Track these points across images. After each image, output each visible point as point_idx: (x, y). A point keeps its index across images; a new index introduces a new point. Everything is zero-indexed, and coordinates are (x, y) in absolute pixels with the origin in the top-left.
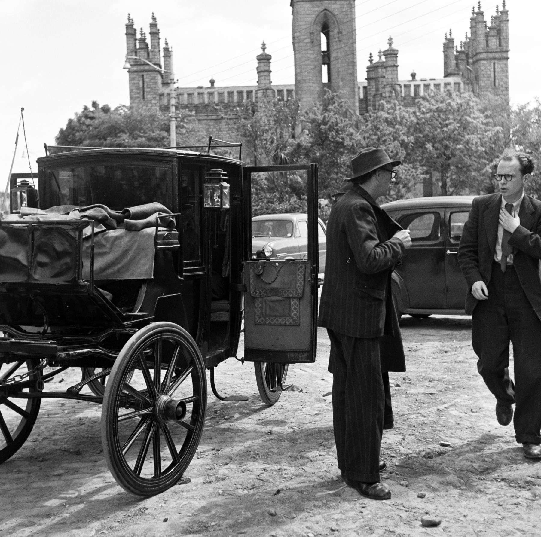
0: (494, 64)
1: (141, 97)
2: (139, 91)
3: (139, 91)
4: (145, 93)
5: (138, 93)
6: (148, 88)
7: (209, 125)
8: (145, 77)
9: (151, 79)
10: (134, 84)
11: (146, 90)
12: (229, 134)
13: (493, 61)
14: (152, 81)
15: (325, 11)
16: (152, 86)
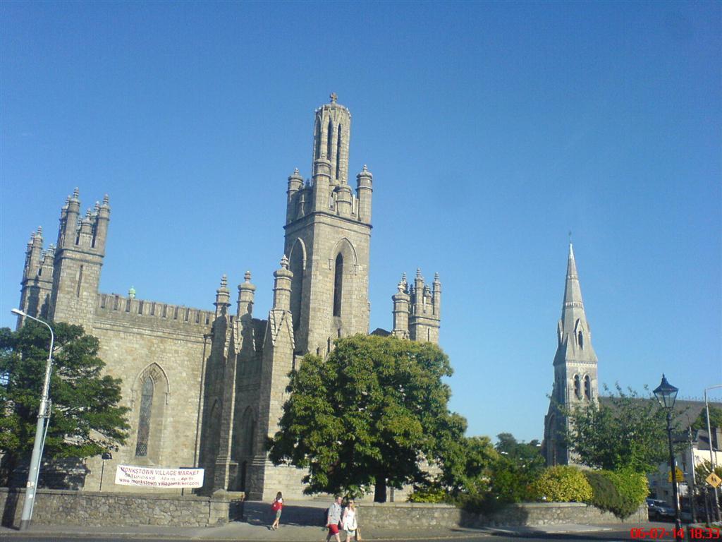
1: (76, 293)
2: (73, 284)
4: (81, 288)
5: (73, 287)
6: (85, 282)
7: (152, 343)
8: (84, 268)
9: (92, 273)
12: (175, 357)
13: (428, 327)
16: (91, 282)
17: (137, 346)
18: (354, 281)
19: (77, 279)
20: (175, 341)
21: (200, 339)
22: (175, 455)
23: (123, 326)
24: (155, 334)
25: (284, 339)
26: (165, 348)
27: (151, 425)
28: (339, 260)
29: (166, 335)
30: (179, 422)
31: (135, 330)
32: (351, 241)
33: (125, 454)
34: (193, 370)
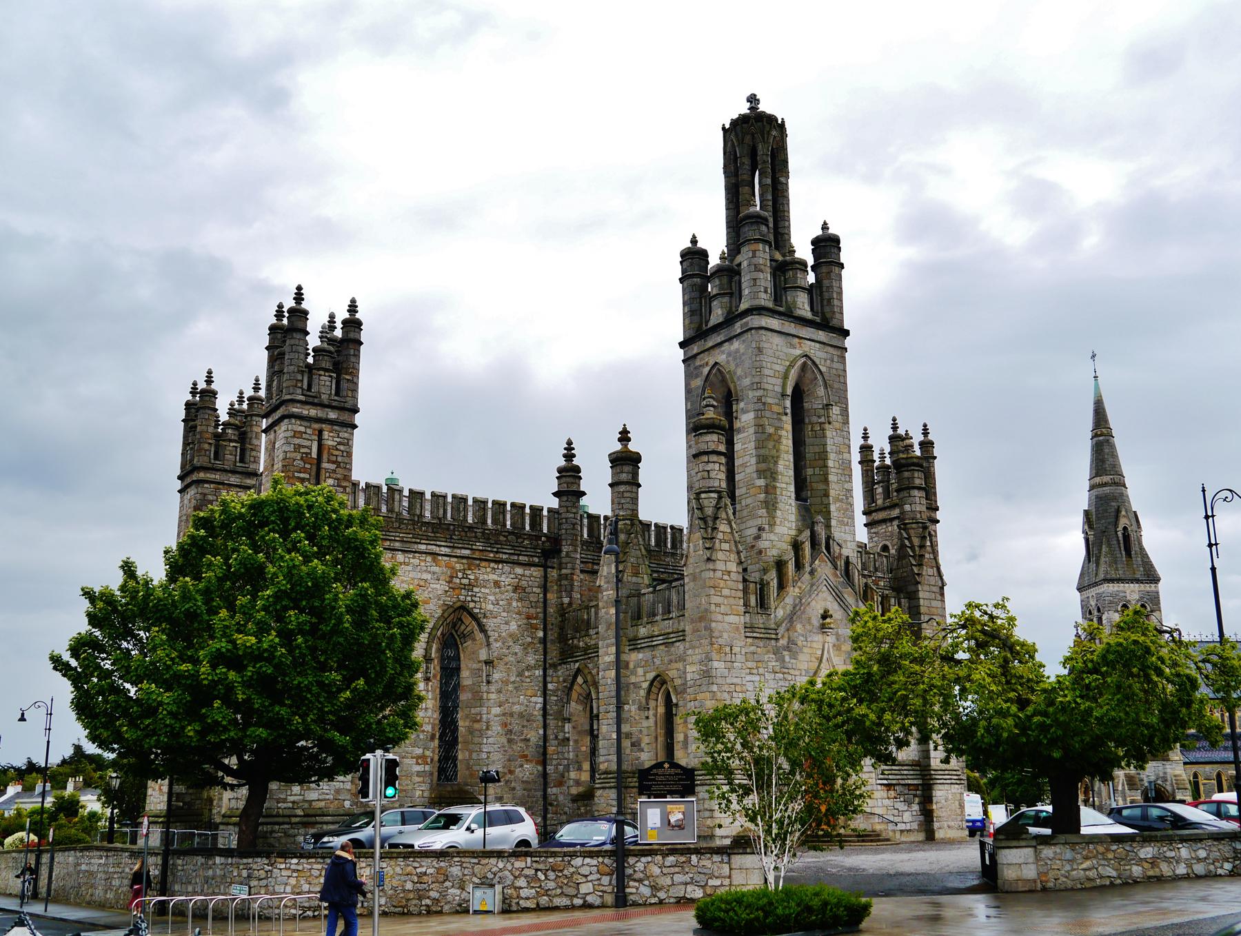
6: (329, 461)
8: (326, 434)
9: (339, 443)
10: (298, 447)
11: (325, 465)
12: (495, 594)
14: (342, 448)
15: (803, 360)
16: (340, 459)
17: (428, 576)
18: (828, 434)
19: (314, 455)
20: (492, 565)
21: (536, 560)
23: (402, 541)
24: (458, 552)
25: (726, 546)
26: (476, 579)
27: (460, 723)
28: (798, 396)
29: (477, 555)
30: (511, 715)
31: (423, 547)
32: (818, 362)
33: (421, 779)
34: (528, 618)
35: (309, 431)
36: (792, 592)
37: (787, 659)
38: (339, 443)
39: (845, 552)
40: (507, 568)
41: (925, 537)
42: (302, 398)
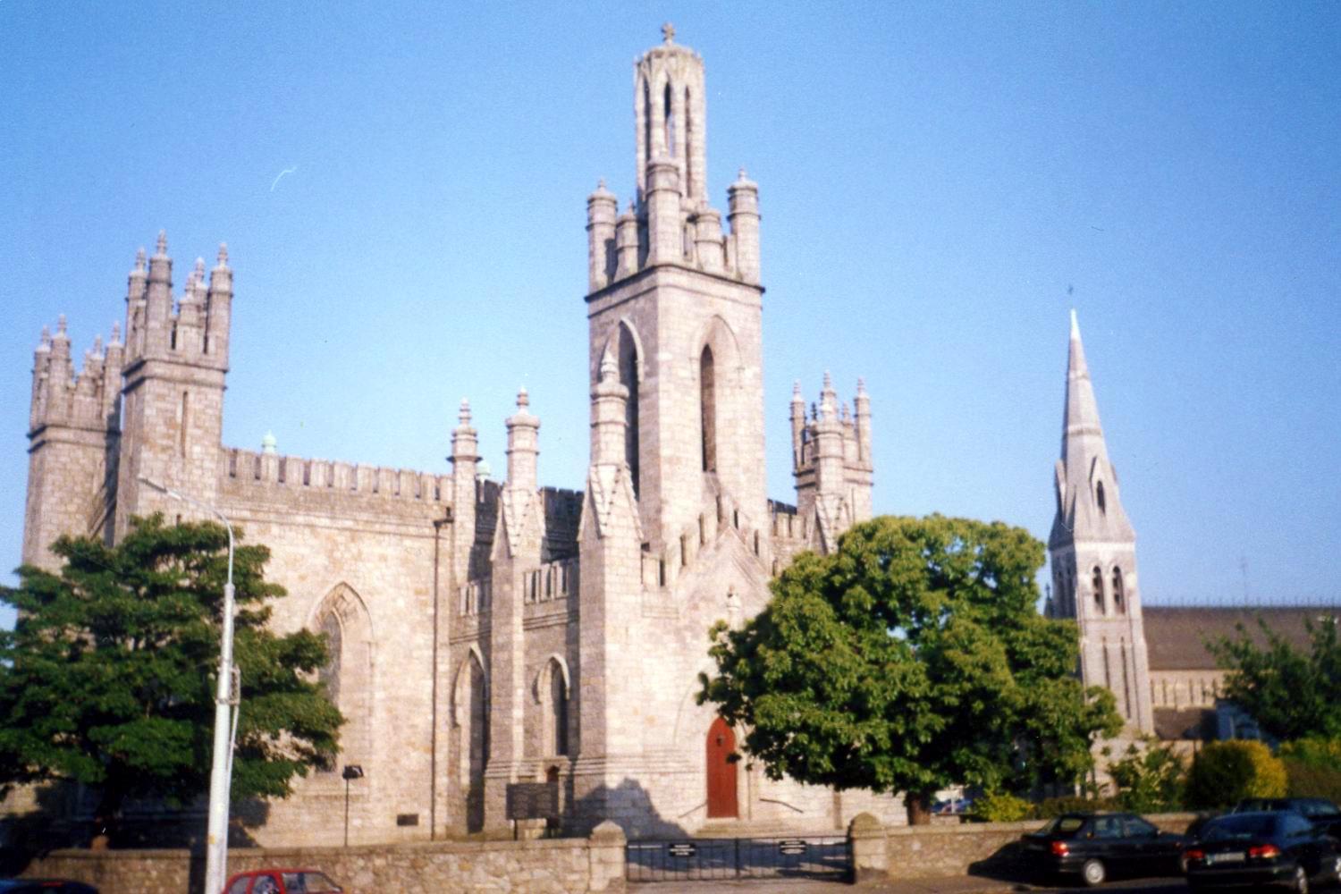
0: (853, 490)
1: (177, 447)
2: (171, 432)
3: (171, 432)
4: (188, 439)
5: (170, 437)
7: (335, 543)
8: (191, 397)
11: (190, 431)
19: (179, 420)
20: (378, 537)
22: (393, 766)
24: (340, 524)
25: (623, 522)
26: (360, 553)
28: (707, 356)
29: (360, 527)
30: (397, 699)
34: (418, 592)
35: (173, 393)
36: (696, 567)
37: (688, 640)
38: (207, 407)
39: (755, 525)
40: (394, 540)
41: (839, 509)
42: (166, 358)
